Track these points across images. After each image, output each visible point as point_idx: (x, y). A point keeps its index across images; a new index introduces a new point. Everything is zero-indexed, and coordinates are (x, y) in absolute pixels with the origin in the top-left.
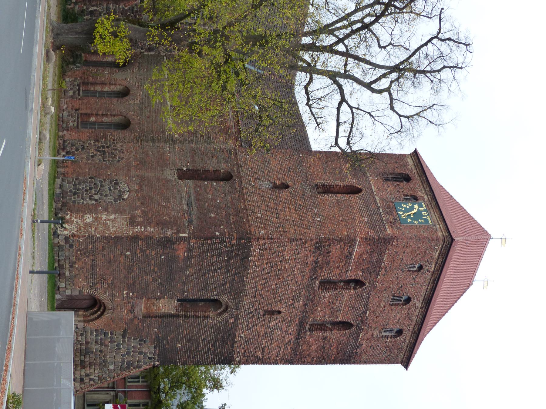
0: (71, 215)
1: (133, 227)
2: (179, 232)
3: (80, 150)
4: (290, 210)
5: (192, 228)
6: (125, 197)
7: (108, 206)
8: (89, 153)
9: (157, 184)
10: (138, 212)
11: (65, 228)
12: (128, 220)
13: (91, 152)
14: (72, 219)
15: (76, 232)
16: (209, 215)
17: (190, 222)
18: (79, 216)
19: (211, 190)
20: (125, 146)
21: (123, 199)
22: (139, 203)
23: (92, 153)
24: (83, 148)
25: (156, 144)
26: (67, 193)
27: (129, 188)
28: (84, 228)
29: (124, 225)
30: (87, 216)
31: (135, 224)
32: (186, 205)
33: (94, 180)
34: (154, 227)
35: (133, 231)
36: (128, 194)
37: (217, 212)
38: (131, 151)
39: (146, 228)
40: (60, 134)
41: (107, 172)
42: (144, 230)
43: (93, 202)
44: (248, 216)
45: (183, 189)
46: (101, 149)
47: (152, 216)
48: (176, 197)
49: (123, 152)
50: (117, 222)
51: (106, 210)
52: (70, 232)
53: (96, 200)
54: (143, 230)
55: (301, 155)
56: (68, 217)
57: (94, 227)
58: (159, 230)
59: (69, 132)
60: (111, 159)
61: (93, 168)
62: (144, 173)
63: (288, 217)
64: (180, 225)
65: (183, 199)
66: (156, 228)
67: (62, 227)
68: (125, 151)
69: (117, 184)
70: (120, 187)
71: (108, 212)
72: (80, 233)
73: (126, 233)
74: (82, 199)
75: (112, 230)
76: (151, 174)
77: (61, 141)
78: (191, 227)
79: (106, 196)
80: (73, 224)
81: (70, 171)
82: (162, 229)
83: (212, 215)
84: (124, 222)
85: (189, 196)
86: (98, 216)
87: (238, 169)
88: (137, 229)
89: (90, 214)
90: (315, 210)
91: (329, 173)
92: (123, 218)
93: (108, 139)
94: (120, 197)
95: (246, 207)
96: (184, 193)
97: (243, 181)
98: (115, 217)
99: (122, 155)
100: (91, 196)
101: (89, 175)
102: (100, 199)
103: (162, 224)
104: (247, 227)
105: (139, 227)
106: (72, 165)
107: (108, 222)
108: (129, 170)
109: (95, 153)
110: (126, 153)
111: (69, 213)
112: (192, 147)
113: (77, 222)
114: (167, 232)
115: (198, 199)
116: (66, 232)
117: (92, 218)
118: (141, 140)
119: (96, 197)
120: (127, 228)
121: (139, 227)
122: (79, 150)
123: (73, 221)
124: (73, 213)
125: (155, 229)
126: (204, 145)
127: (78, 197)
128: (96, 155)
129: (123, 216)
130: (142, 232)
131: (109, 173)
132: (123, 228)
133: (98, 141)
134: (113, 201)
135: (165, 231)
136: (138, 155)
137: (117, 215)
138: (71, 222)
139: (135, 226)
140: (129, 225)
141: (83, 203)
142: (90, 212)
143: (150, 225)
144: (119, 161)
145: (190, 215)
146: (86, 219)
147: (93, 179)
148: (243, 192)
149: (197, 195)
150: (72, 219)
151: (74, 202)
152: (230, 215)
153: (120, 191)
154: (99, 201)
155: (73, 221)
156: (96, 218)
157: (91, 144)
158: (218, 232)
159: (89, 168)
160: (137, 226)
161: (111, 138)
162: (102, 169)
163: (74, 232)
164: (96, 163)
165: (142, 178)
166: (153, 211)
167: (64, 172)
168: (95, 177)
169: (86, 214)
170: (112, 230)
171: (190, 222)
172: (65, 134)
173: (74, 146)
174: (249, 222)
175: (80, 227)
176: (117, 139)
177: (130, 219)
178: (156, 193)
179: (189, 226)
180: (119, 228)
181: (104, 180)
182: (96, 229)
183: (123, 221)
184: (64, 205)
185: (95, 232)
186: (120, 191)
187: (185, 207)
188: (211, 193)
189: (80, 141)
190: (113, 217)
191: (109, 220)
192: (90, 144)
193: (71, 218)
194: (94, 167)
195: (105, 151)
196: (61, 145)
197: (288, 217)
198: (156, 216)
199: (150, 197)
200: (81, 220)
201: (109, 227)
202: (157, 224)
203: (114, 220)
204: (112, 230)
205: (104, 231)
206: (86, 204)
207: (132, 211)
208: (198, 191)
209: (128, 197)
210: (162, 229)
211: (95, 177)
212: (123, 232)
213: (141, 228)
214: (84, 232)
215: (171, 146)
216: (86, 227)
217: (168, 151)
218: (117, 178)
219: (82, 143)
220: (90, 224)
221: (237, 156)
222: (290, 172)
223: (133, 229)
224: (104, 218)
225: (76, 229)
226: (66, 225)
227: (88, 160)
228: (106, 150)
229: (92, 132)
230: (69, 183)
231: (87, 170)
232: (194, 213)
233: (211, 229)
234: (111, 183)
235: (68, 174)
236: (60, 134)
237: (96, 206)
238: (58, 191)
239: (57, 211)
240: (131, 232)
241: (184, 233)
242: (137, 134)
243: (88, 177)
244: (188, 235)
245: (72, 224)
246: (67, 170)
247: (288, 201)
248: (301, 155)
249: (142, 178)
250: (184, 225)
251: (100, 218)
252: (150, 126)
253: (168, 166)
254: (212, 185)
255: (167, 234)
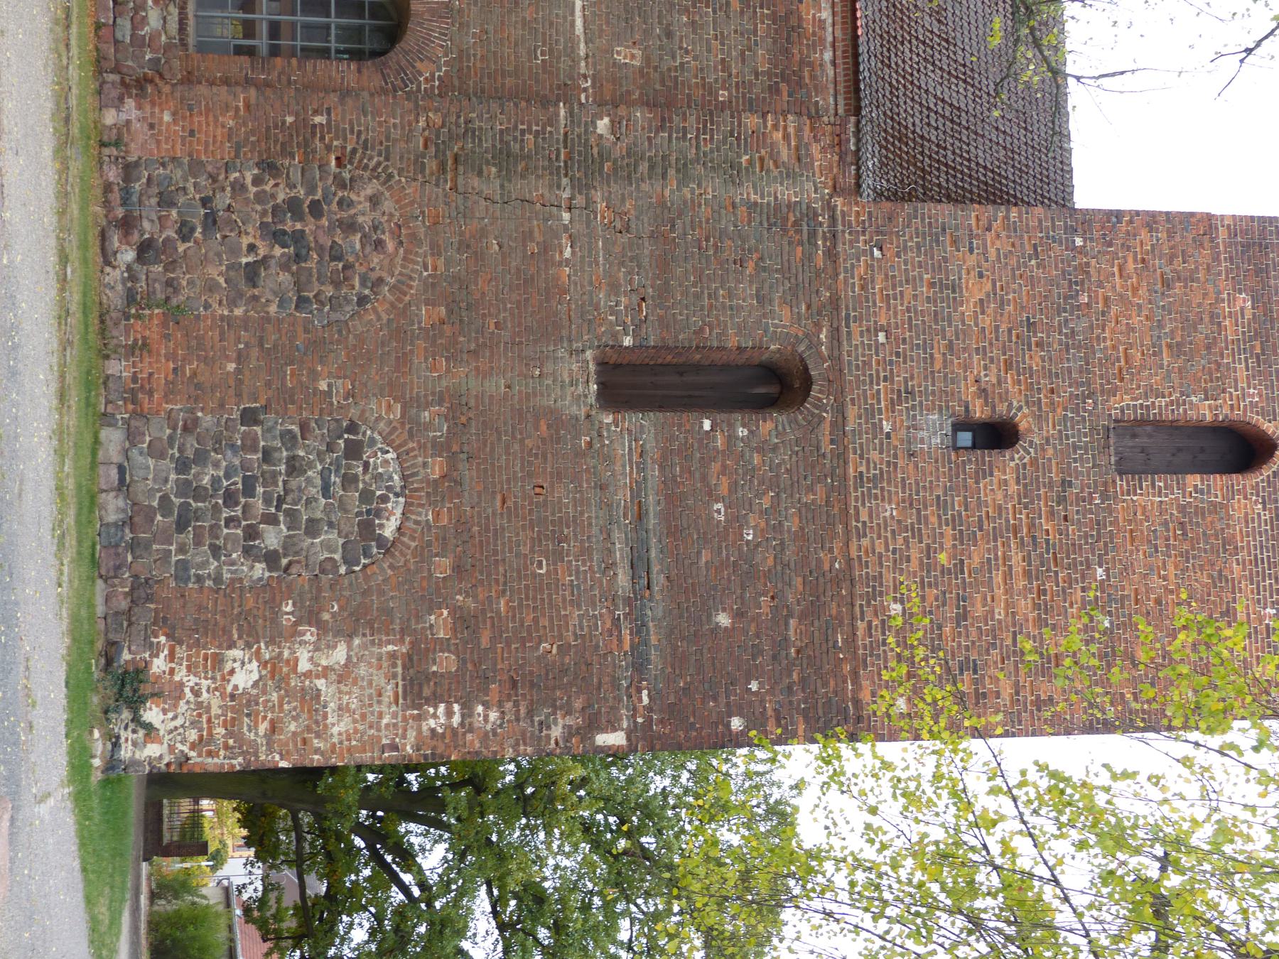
0: (172, 657)
1: (419, 707)
2: (594, 724)
3: (198, 234)
4: (1008, 575)
5: (646, 700)
6: (389, 529)
7: (319, 590)
8: (235, 251)
9: (517, 447)
10: (440, 622)
11: (149, 728)
12: (399, 670)
13: (245, 241)
14: (177, 678)
15: (193, 747)
16: (709, 616)
17: (639, 666)
18: (206, 659)
19: (724, 470)
20: (388, 205)
21: (381, 540)
22: (442, 566)
23: (252, 248)
24: (211, 221)
25: (518, 187)
26: (149, 515)
27: (404, 478)
28: (225, 726)
29: (385, 700)
30: (236, 653)
31: (427, 692)
32: (628, 567)
33: (258, 429)
34: (500, 704)
35: (419, 731)
36: (399, 511)
37: (742, 598)
38: (413, 236)
39: (471, 715)
40: (110, 117)
41: (315, 376)
42: (462, 724)
43: (260, 570)
44: (853, 618)
45: (618, 468)
46: (289, 225)
47: (493, 640)
48: (590, 524)
49: (379, 244)
50: (355, 683)
51: (310, 616)
52: (171, 749)
53: (271, 559)
54: (456, 720)
55: (1079, 242)
56: (159, 665)
57: (265, 718)
58: (518, 720)
59: (148, 108)
60: (329, 291)
61: (255, 352)
62: (462, 376)
63: (1000, 613)
64: (600, 682)
65: (617, 535)
66: (509, 705)
67: (136, 719)
68: (386, 237)
69: (354, 451)
70: (366, 465)
71: (322, 627)
72: (210, 754)
73: (394, 747)
74: (216, 551)
75: (335, 730)
76: (495, 386)
77: (113, 174)
78: (639, 691)
79: (312, 528)
80: (182, 706)
81: (159, 369)
82: (530, 714)
83: (724, 620)
84: (383, 682)
85: (641, 516)
86: (281, 654)
87: (835, 334)
88: (435, 716)
89: (248, 646)
90: (1100, 571)
91: (1169, 346)
92: (380, 659)
93: (314, 151)
94: (368, 529)
95: (849, 561)
96: (622, 496)
97: (852, 412)
98: (349, 658)
99: (376, 260)
100: (252, 533)
101: (239, 395)
102: (288, 544)
103: (532, 685)
104: (845, 682)
105: (442, 708)
106: (167, 337)
107: (321, 683)
108: (403, 361)
109: (262, 252)
110: (390, 246)
111: (163, 639)
112: (662, 204)
113: (197, 693)
114: (549, 728)
115: (673, 531)
116: (153, 750)
117: (255, 664)
118: (456, 159)
119: (272, 538)
120: (395, 715)
121: (442, 708)
122: (193, 230)
123: (181, 685)
124: (180, 643)
125: (503, 713)
126: (712, 188)
127: (198, 542)
128: (265, 261)
129: (380, 645)
130: (454, 732)
131: (323, 386)
132: (381, 715)
133: (269, 167)
134: (337, 557)
135: (541, 723)
136: (441, 262)
137: (357, 641)
138: (170, 694)
139: (428, 701)
140: (405, 699)
141: (218, 579)
142: (250, 638)
143: (486, 691)
144: (362, 300)
145: (640, 629)
146: (232, 672)
147: (256, 422)
148: (845, 477)
149: (672, 498)
150: (177, 678)
151: (183, 566)
152: (790, 615)
153: (366, 496)
154: (284, 561)
155: (181, 685)
156: (274, 666)
157: (243, 187)
158: (741, 715)
159: (239, 352)
160: (435, 700)
161: (329, 148)
162: (292, 363)
163: (185, 749)
164: (268, 319)
165: (455, 405)
166: (498, 612)
167: (134, 379)
168: (266, 408)
169: (232, 645)
170: (335, 730)
171: (639, 666)
172: (128, 122)
173: (172, 204)
174: (856, 648)
175: (209, 721)
176: (354, 151)
177: (409, 661)
178: (510, 503)
179: (633, 690)
180: (363, 716)
181: (304, 427)
182: (273, 728)
183: (379, 679)
184: (142, 590)
185: (270, 749)
186: (366, 496)
187: (623, 579)
188: (724, 489)
189: (195, 167)
190: (339, 654)
191: (327, 670)
192: (238, 187)
193: (172, 671)
194: (261, 345)
195: (303, 231)
196: (116, 196)
197: (1000, 613)
198: (508, 644)
199: (487, 530)
200: (213, 678)
201: (325, 717)
202: (514, 684)
203: (344, 675)
204: (339, 727)
205: (304, 741)
206: (233, 580)
207: (419, 618)
208: (674, 476)
209: (399, 529)
210: (530, 714)
211: (266, 408)
212: (379, 738)
213: (449, 714)
214: (226, 747)
215: (580, 200)
216: (233, 719)
217: (566, 228)
218: (354, 412)
219: (203, 181)
220: (248, 704)
221: (836, 255)
222: (1029, 345)
223: (419, 715)
224: (304, 666)
225: (193, 735)
226: (152, 714)
227: (232, 304)
228: (309, 226)
229: (248, 106)
230: (156, 451)
231: (231, 367)
232: (656, 609)
233: (715, 699)
234: (330, 448)
235: (150, 393)
236: (110, 117)
237: (270, 594)
238: (113, 508)
239: (111, 636)
240: (412, 735)
241: (614, 730)
242: (439, 121)
243: (236, 415)
244: (629, 739)
245: (175, 706)
246: (145, 368)
247: (1007, 520)
248: (1079, 242)
249: (455, 405)
250: (615, 684)
251: (288, 661)
252: (491, 28)
253: (564, 333)
254: (731, 439)
255: (548, 737)
